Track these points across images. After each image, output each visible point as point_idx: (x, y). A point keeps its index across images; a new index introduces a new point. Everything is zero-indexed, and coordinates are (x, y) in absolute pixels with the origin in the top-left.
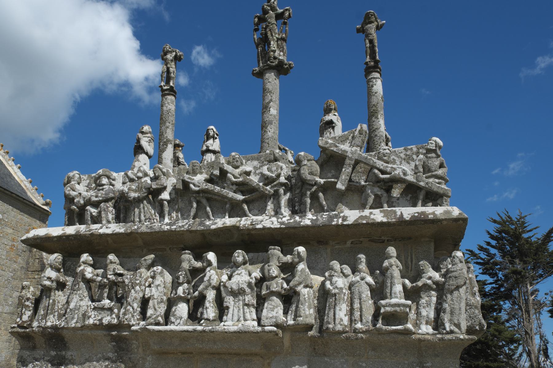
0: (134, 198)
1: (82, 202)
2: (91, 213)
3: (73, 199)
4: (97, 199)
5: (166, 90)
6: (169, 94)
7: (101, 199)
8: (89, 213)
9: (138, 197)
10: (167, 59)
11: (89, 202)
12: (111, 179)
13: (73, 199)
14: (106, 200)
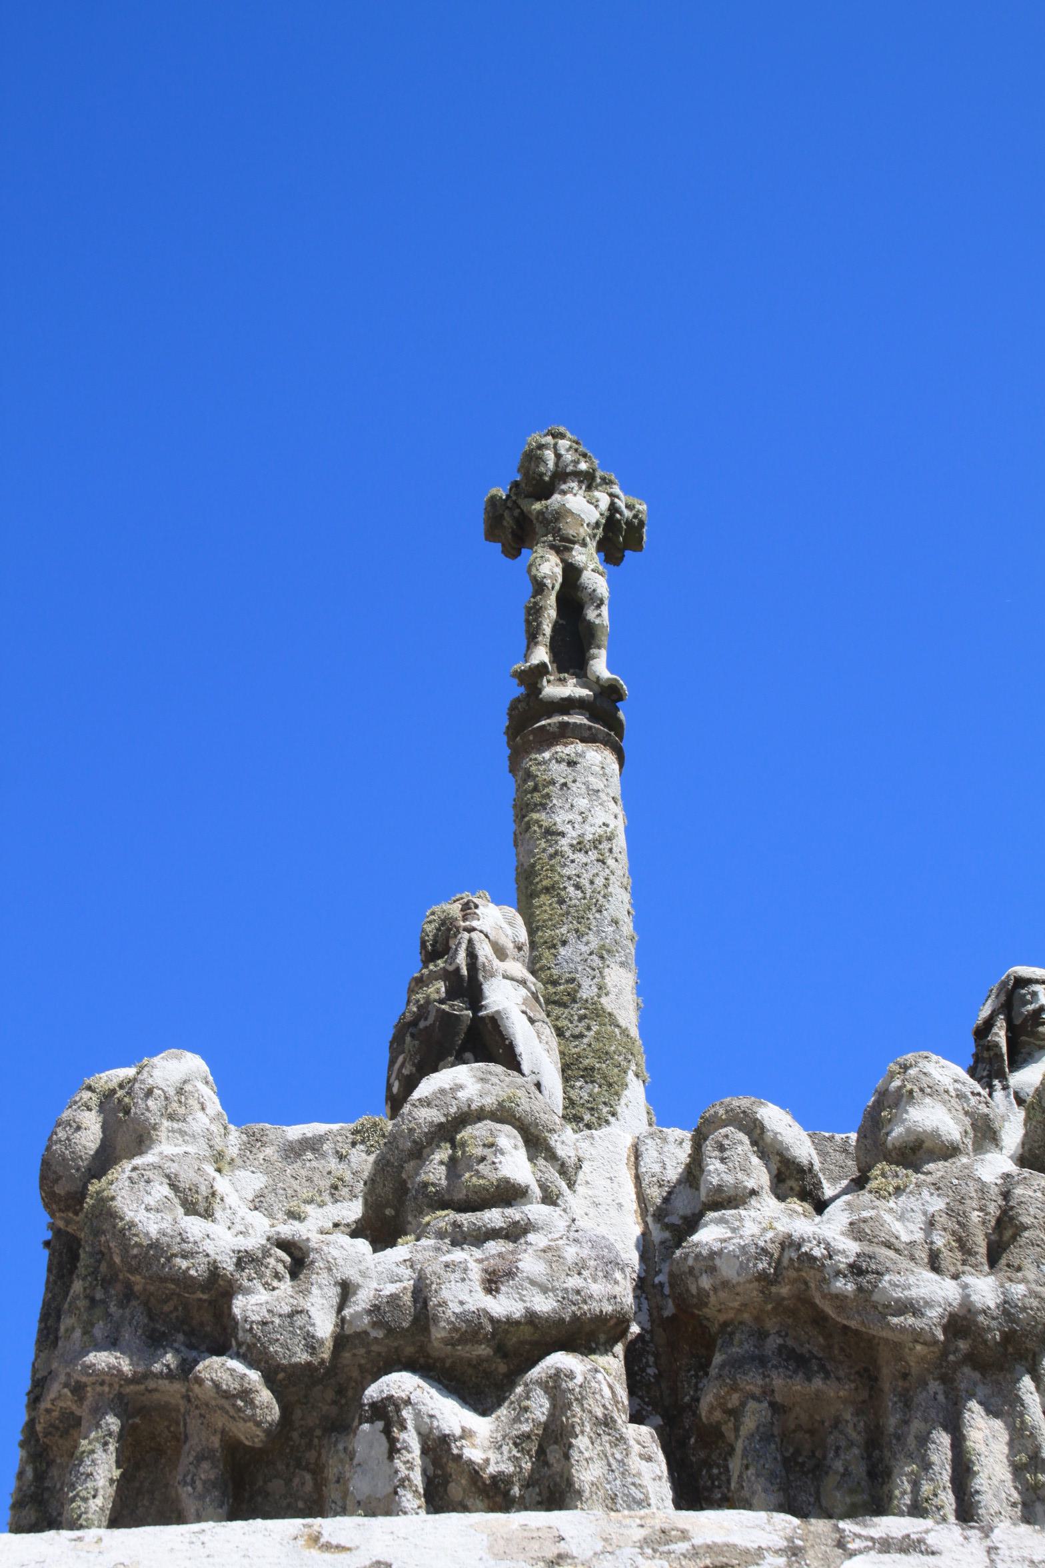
0: (961, 1322)
1: (324, 1326)
2: (438, 1448)
3: (219, 1288)
4: (504, 1306)
5: (567, 705)
6: (589, 738)
7: (544, 1305)
8: (410, 1438)
9: (1007, 1308)
10: (561, 514)
11: (409, 1335)
12: (552, 1156)
13: (219, 1288)
14: (584, 1333)
